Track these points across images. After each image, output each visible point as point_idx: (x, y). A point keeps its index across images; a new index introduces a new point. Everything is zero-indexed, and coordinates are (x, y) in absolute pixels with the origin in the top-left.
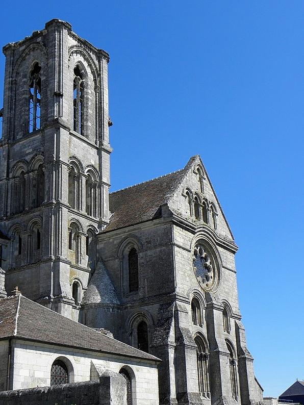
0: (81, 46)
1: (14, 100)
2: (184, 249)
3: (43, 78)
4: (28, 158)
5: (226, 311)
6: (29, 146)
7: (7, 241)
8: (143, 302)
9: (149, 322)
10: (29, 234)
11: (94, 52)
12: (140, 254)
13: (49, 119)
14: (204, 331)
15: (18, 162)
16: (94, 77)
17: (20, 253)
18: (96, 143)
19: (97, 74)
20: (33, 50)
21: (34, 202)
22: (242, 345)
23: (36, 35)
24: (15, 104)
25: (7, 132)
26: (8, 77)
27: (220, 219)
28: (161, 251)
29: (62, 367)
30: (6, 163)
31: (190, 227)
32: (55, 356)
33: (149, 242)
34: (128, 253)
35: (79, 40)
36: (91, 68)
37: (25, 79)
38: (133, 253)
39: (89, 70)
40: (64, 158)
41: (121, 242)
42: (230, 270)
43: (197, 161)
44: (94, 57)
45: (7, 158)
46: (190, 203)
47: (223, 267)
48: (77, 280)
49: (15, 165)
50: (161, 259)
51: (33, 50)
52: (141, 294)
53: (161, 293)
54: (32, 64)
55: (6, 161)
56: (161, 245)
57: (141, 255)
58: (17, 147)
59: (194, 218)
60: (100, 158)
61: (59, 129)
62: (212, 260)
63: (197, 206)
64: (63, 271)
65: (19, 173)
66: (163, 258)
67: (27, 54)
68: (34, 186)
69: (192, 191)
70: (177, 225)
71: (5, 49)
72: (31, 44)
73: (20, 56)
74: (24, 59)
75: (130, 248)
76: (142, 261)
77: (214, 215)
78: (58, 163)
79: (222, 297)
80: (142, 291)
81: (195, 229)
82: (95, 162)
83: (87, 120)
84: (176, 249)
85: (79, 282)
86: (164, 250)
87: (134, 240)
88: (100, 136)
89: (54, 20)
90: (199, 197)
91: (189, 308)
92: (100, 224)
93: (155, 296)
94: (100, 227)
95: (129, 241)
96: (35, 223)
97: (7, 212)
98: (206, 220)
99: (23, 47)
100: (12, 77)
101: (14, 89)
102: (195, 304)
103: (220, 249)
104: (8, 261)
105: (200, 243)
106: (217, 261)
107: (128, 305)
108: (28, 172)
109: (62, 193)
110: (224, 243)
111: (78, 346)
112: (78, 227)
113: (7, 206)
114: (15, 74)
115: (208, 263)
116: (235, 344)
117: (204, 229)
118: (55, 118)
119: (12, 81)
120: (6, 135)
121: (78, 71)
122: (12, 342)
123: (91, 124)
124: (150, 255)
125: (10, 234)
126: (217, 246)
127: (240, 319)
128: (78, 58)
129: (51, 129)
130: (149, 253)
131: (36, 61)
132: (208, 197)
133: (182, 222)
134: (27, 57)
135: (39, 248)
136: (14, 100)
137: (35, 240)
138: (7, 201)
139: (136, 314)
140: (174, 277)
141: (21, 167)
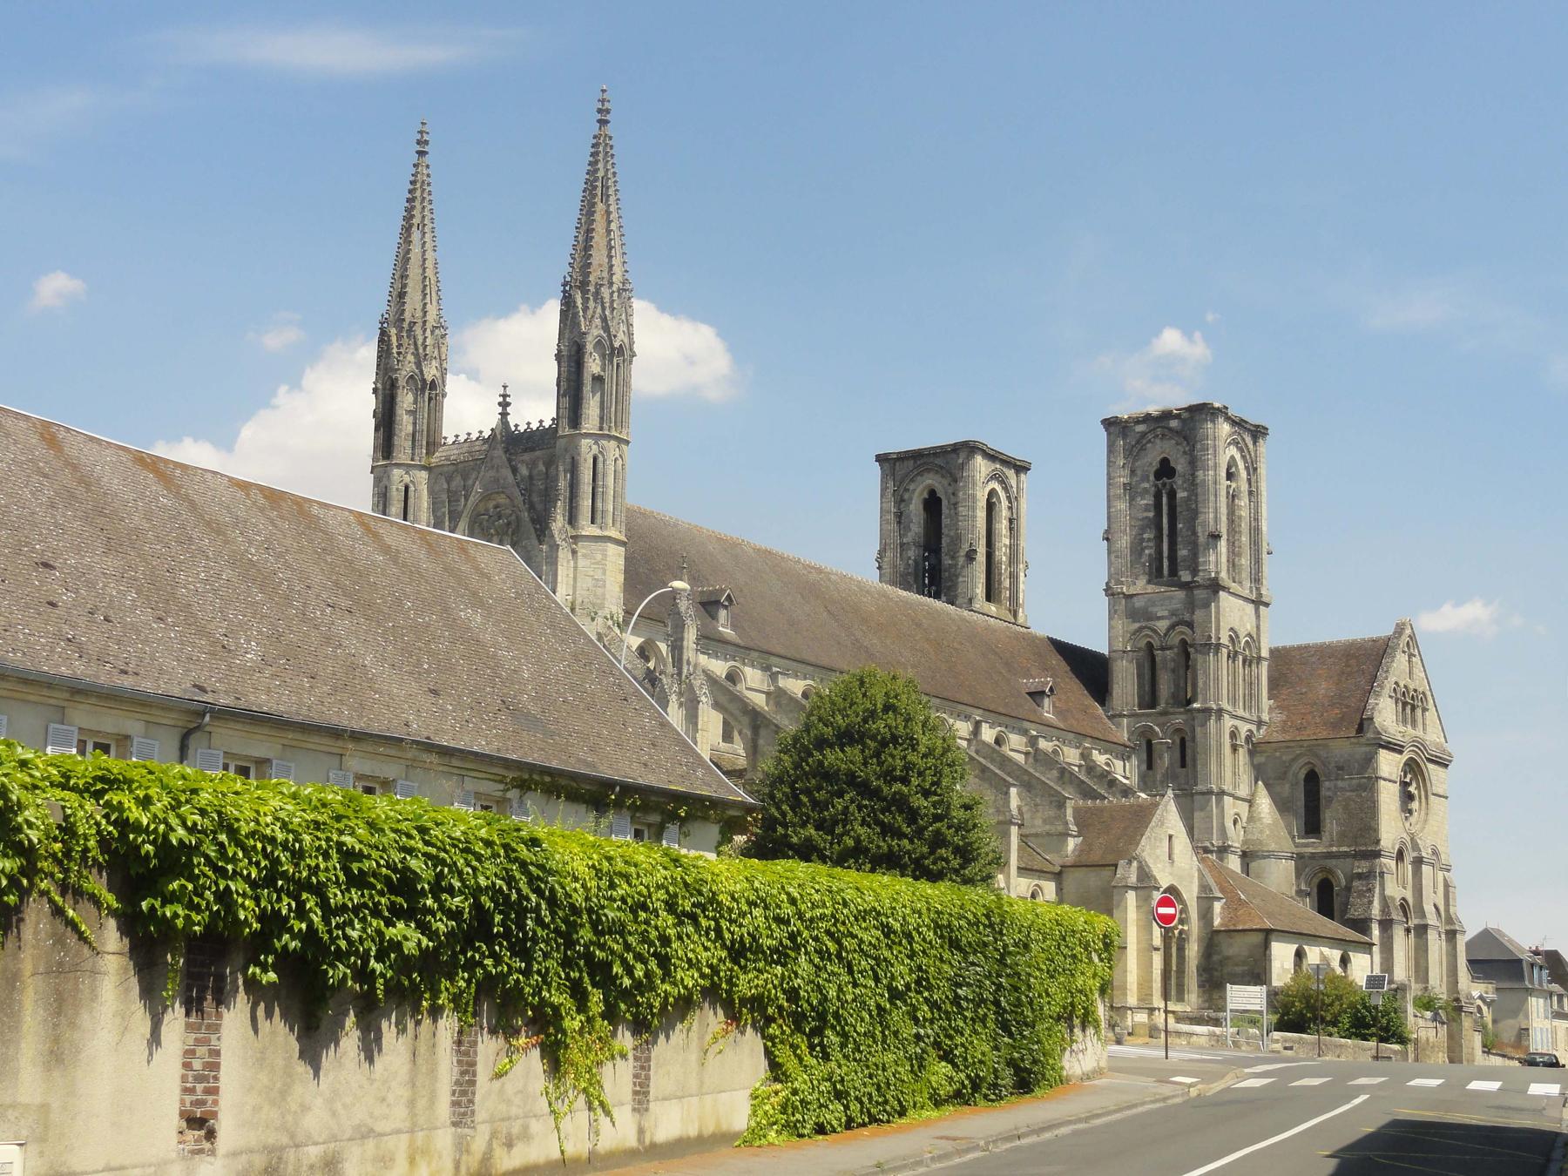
3: (1181, 494)
13: (1201, 574)
16: (1249, 474)
18: (1251, 592)
19: (1252, 469)
20: (1161, 439)
22: (1452, 910)
23: (1166, 415)
27: (1431, 715)
29: (1300, 955)
32: (1296, 946)
33: (1340, 768)
34: (1303, 776)
36: (1246, 462)
37: (1146, 485)
41: (1294, 760)
42: (1440, 796)
46: (1396, 703)
47: (1434, 794)
63: (1405, 704)
65: (1142, 643)
67: (1149, 441)
71: (1109, 424)
73: (1138, 442)
74: (1143, 449)
79: (1429, 843)
81: (1403, 747)
83: (1239, 555)
89: (1204, 405)
92: (1260, 723)
99: (1141, 428)
103: (1431, 766)
106: (1425, 785)
108: (1163, 649)
110: (1436, 756)
116: (1442, 909)
122: (1268, 934)
123: (1245, 561)
127: (1448, 870)
128: (1233, 451)
129: (1205, 591)
133: (1390, 743)
134: (1149, 445)
135: (1183, 765)
141: (1147, 636)
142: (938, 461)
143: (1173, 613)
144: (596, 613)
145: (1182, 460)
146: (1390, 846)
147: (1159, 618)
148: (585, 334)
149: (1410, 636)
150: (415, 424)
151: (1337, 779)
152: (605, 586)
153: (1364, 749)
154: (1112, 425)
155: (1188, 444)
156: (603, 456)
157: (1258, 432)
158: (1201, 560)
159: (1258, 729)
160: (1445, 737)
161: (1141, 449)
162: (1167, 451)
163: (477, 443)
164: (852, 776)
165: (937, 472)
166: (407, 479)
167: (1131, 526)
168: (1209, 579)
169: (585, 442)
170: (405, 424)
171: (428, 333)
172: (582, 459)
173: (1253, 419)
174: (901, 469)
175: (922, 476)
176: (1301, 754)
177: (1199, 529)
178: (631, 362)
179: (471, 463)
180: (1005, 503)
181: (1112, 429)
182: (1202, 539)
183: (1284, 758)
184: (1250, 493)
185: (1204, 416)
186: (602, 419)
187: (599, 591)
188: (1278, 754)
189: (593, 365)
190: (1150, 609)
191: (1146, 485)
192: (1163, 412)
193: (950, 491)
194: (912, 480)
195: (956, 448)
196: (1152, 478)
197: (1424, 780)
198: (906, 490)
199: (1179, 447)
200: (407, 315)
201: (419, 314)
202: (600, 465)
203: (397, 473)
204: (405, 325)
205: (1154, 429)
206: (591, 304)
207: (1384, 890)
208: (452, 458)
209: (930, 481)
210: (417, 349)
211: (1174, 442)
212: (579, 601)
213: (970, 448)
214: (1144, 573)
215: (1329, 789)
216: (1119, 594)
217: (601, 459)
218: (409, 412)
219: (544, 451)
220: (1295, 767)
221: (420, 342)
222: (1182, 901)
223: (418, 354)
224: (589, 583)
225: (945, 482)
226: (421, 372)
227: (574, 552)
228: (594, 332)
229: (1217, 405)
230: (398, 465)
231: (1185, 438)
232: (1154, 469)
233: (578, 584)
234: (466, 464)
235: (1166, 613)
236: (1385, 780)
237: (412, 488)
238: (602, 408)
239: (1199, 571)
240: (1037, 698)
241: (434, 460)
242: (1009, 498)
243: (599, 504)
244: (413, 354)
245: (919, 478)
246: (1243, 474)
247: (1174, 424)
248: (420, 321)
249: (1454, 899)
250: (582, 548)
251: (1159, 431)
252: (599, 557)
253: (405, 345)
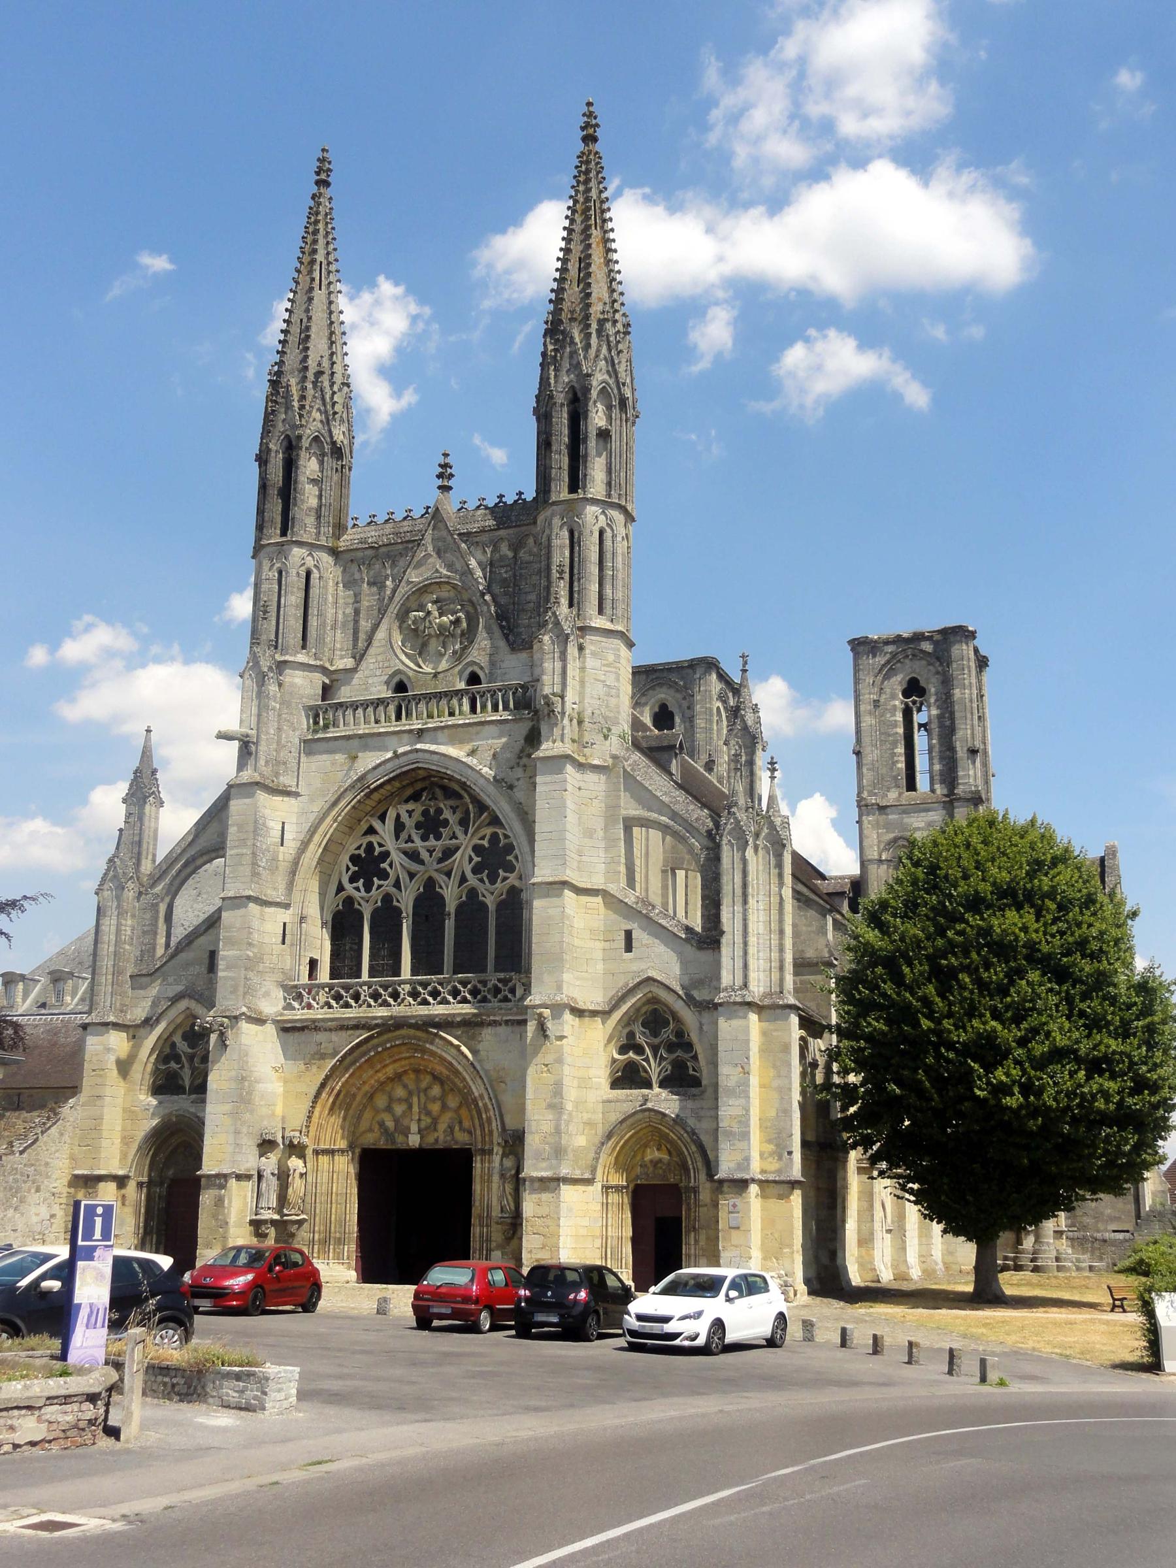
13: (961, 787)
20: (911, 660)
23: (918, 637)
54: (907, 678)
67: (899, 661)
89: (960, 627)
134: (899, 665)
142: (674, 677)
144: (609, 730)
145: (934, 680)
148: (589, 375)
150: (320, 497)
152: (618, 696)
155: (941, 664)
156: (612, 530)
158: (960, 773)
162: (918, 671)
163: (405, 523)
164: (1032, 946)
165: (671, 687)
166: (310, 562)
167: (881, 741)
168: (971, 792)
169: (591, 510)
170: (308, 496)
171: (336, 388)
172: (588, 531)
175: (654, 690)
177: (958, 745)
178: (634, 423)
179: (400, 547)
181: (861, 649)
182: (961, 753)
185: (958, 638)
186: (609, 484)
187: (613, 701)
189: (598, 418)
192: (915, 634)
193: (685, 704)
195: (693, 664)
199: (931, 668)
200: (312, 363)
201: (326, 364)
202: (608, 543)
203: (297, 552)
204: (310, 375)
206: (594, 340)
208: (370, 540)
209: (663, 696)
210: (324, 404)
211: (924, 662)
212: (588, 712)
216: (873, 805)
217: (608, 533)
218: (314, 481)
219: (511, 531)
221: (328, 397)
223: (326, 412)
224: (600, 690)
225: (679, 696)
226: (330, 432)
227: (581, 648)
228: (599, 378)
229: (970, 629)
230: (300, 544)
231: (938, 659)
233: (588, 690)
234: (390, 548)
235: (922, 825)
237: (315, 574)
238: (609, 471)
239: (958, 784)
240: (837, 900)
241: (344, 543)
243: (608, 591)
244: (319, 410)
245: (651, 692)
247: (927, 647)
248: (328, 372)
250: (590, 641)
252: (611, 658)
253: (309, 398)
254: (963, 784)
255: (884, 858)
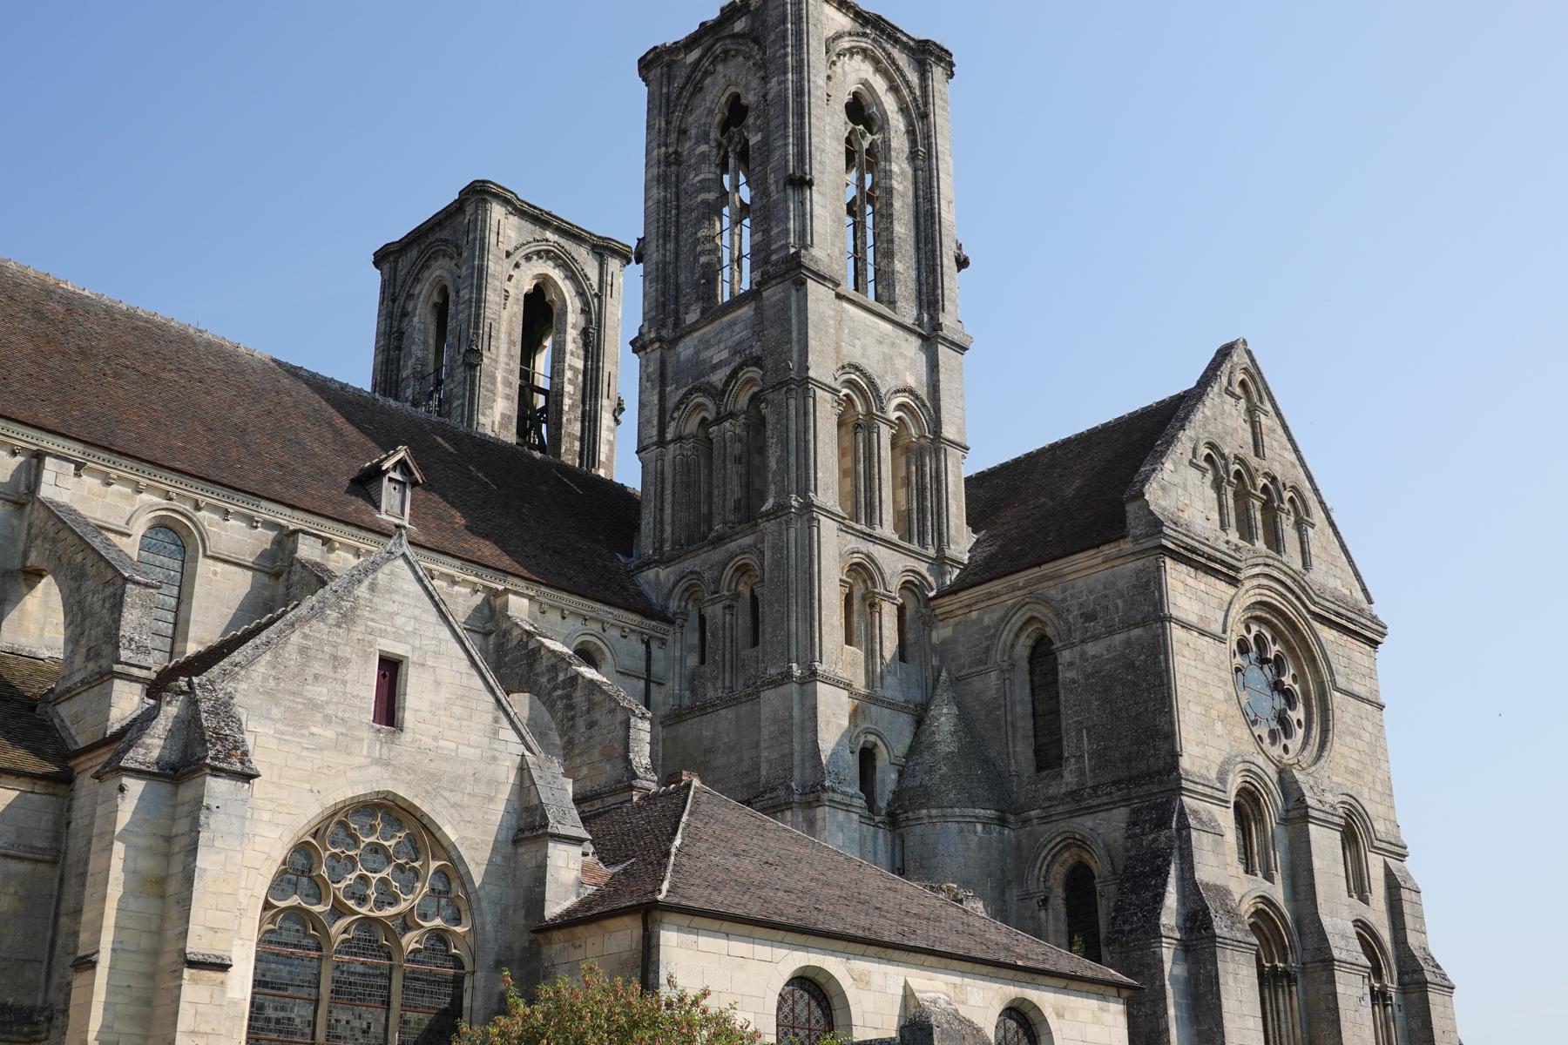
0: (865, 35)
1: (673, 212)
2: (1202, 633)
3: (755, 139)
4: (718, 378)
5: (1353, 833)
6: (719, 342)
7: (665, 626)
8: (1078, 802)
9: (1100, 867)
10: (728, 602)
11: (905, 47)
12: (1064, 653)
13: (774, 257)
14: (1277, 892)
15: (690, 392)
17: (702, 661)
19: (919, 115)
21: (737, 508)
22: (1412, 939)
24: (677, 221)
25: (657, 307)
26: (655, 144)
28: (1128, 643)
30: (655, 399)
31: (1223, 563)
33: (1089, 617)
34: (1026, 652)
35: (859, 16)
37: (703, 148)
38: (1042, 653)
39: (889, 103)
40: (821, 367)
41: (1005, 619)
42: (1362, 700)
43: (1238, 357)
44: (902, 59)
45: (657, 383)
48: (872, 738)
49: (681, 402)
50: (1131, 666)
51: (725, 60)
52: (1069, 778)
53: (1135, 773)
54: (723, 100)
55: (657, 390)
56: (1128, 625)
57: (1066, 656)
58: (686, 349)
59: (1234, 536)
60: (933, 367)
61: (804, 283)
62: (1299, 666)
63: (1242, 497)
64: (829, 712)
65: (692, 426)
66: (1137, 663)
67: (707, 73)
68: (738, 460)
69: (1226, 451)
70: (1178, 557)
72: (717, 41)
75: (1033, 635)
76: (1071, 674)
77: (1300, 525)
78: (803, 384)
80: (1073, 767)
81: (1238, 570)
82: (918, 380)
84: (1177, 633)
85: (880, 743)
86: (1139, 638)
87: (1045, 610)
88: (930, 297)
90: (1248, 470)
91: (1226, 819)
93: (1115, 783)
94: (940, 574)
95: (1029, 614)
96: (744, 570)
97: (662, 542)
98: (1275, 542)
99: (694, 55)
100: (666, 145)
101: (673, 179)
102: (1247, 808)
103: (1327, 634)
104: (670, 684)
105: (1264, 613)
107: (1033, 813)
108: (719, 420)
109: (819, 475)
110: (1338, 614)
111: (860, 933)
112: (872, 578)
113: (662, 523)
114: (674, 136)
115: (1287, 680)
116: (1385, 935)
117: (1267, 570)
118: (792, 250)
119: (667, 156)
120: (653, 314)
121: (858, 110)
123: (904, 267)
124: (1094, 657)
125: (673, 605)
126: (1316, 625)
129: (780, 287)
130: (1091, 649)
131: (733, 89)
132: (1277, 470)
133: (1194, 550)
134: (708, 81)
135: (755, 643)
136: (673, 212)
137: (744, 620)
138: (662, 510)
139: (1058, 839)
140: (1172, 724)
142: (445, 234)
143: (735, 351)
146: (1213, 775)
147: (715, 368)
149: (1246, 370)
151: (1083, 641)
153: (1132, 566)
154: (653, 64)
157: (928, 54)
159: (940, 574)
160: (1364, 590)
161: (693, 94)
173: (916, 28)
174: (404, 264)
175: (428, 267)
176: (1014, 605)
180: (573, 305)
183: (986, 620)
184: (913, 156)
188: (974, 615)
190: (704, 355)
191: (703, 148)
194: (417, 280)
196: (714, 134)
197: (1313, 660)
198: (410, 296)
205: (709, 49)
207: (1192, 868)
209: (438, 273)
211: (741, 59)
213: (478, 193)
214: (697, 300)
215: (1071, 664)
220: (1007, 636)
222: (440, 846)
231: (756, 41)
232: (718, 118)
235: (725, 355)
236: (1186, 626)
242: (581, 294)
245: (426, 274)
246: (897, 122)
247: (740, 25)
249: (1420, 917)
251: (718, 48)
254: (776, 251)
255: (669, 436)
